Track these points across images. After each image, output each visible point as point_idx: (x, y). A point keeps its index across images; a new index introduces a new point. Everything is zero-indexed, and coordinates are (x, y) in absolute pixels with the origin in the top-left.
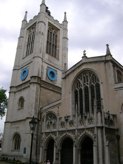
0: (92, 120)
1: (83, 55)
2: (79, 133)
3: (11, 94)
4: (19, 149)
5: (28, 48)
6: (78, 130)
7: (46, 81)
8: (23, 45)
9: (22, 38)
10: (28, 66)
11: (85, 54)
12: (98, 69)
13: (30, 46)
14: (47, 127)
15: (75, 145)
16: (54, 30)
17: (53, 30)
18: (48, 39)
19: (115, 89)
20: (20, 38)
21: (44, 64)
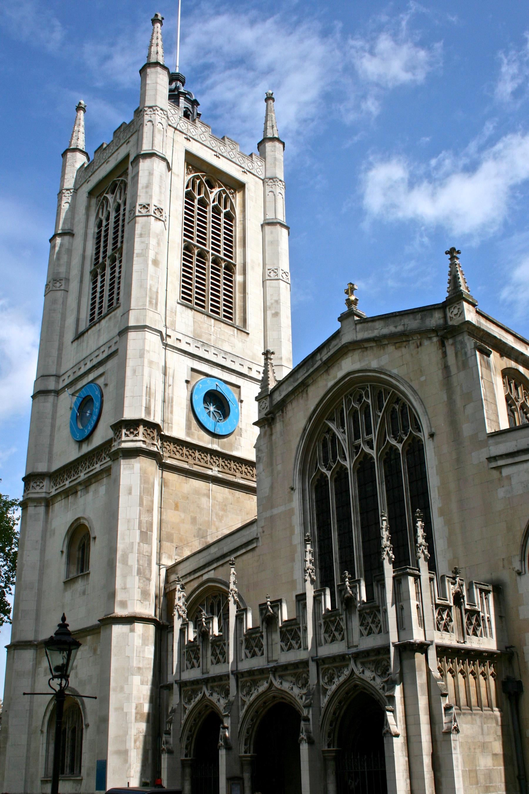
0: (375, 616)
1: (345, 309)
2: (323, 678)
3: (31, 510)
4: (76, 771)
5: (99, 284)
6: (320, 662)
7: (189, 440)
8: (75, 272)
10: (100, 370)
13: (108, 277)
14: (189, 660)
15: (308, 731)
16: (216, 190)
17: (212, 187)
18: (188, 232)
19: (492, 459)
21: (174, 358)
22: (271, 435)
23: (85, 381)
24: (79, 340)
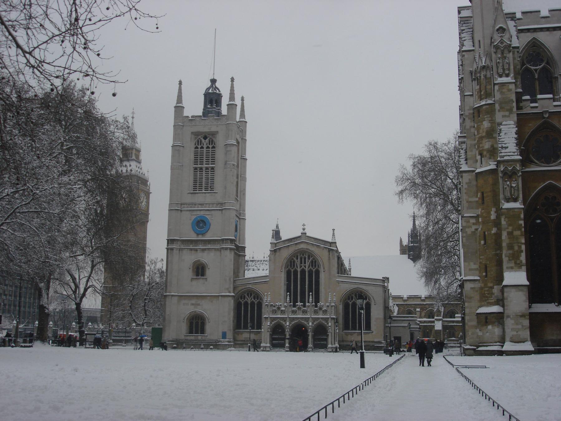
1: (302, 231)
9: (182, 147)
10: (208, 213)
11: (304, 229)
12: (322, 255)
20: (179, 147)
22: (275, 255)
23: (198, 213)
24: (193, 194)
